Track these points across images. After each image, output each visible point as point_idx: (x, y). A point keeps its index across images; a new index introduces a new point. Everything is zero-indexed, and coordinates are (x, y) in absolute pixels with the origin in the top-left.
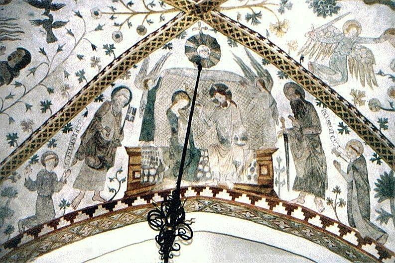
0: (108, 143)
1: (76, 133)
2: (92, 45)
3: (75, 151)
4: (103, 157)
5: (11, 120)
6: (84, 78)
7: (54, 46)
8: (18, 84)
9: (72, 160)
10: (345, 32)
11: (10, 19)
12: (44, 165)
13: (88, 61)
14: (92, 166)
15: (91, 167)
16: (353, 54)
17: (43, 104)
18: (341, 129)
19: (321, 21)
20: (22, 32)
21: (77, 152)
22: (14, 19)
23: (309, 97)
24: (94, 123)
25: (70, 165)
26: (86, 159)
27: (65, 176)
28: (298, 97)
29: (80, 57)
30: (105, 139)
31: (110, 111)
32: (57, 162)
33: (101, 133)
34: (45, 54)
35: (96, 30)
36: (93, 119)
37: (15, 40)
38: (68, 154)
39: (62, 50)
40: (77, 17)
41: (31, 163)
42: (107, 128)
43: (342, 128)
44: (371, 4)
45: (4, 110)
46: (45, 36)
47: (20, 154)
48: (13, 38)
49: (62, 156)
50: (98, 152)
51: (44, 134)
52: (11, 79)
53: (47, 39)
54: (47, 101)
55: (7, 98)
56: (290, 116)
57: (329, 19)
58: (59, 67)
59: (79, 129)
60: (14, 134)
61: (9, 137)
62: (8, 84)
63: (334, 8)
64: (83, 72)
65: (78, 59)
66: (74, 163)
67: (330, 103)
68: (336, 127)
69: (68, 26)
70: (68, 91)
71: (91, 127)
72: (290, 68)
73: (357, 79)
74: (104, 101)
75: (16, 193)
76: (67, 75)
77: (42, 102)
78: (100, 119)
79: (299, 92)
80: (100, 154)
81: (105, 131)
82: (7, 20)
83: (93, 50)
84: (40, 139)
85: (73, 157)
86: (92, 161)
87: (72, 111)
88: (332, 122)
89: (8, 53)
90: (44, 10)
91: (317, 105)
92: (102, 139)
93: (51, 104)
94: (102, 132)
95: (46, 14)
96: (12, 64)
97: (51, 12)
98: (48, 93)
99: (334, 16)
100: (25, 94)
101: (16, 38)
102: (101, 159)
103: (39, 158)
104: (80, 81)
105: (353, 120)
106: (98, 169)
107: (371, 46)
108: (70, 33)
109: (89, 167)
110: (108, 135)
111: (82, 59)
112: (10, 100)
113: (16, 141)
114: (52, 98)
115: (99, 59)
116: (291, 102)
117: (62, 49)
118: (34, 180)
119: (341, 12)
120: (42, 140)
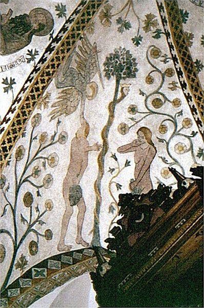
10: (91, 85)
16: (75, 93)
18: (7, 82)
19: (102, 59)
23: (39, 44)
28: (35, 26)
43: (9, 83)
44: (109, 109)
56: (11, 11)
57: (102, 68)
63: (109, 74)
67: (49, 70)
68: (8, 74)
72: (82, 25)
73: (57, 99)
79: (44, 28)
88: (14, 69)
91: (28, 51)
99: (103, 74)
105: (35, 99)
107: (78, 112)
116: (28, 16)
119: (105, 80)
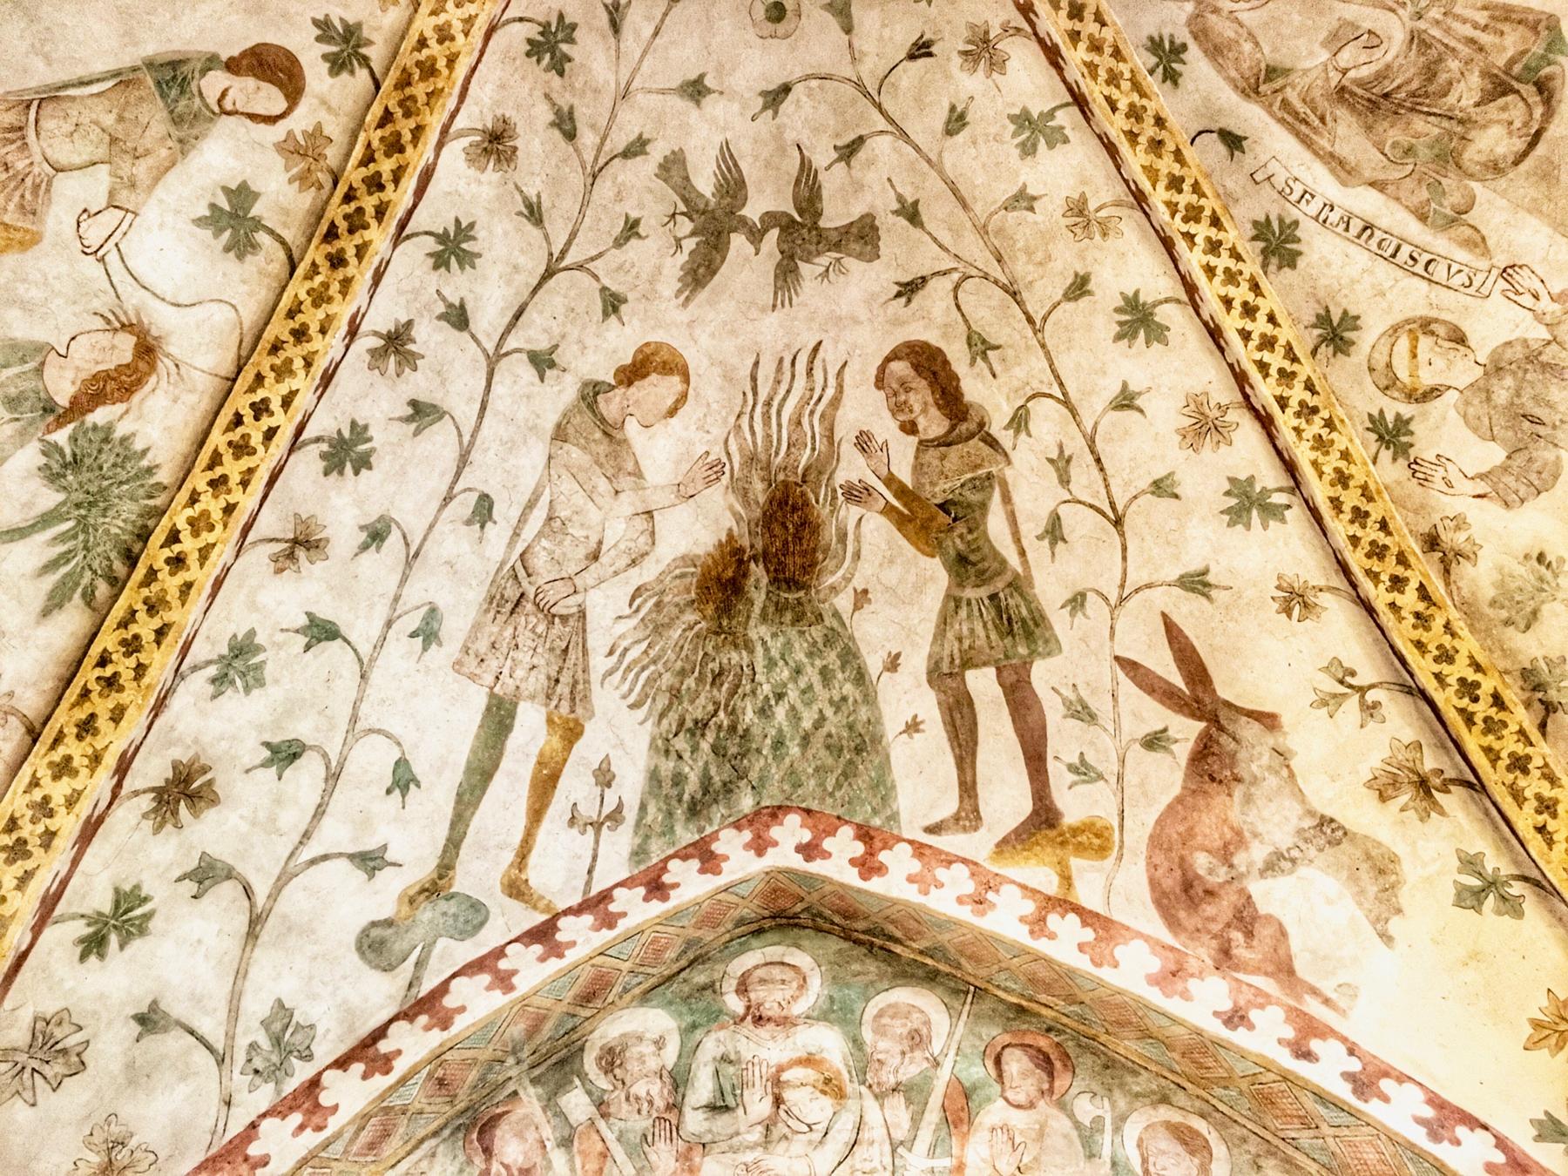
0: (1417, 40)
1: (1313, 208)
2: (912, 57)
3: (1414, 229)
4: (1485, 74)
5: (1162, 488)
6: (1051, 114)
7: (893, 228)
8: (1019, 421)
9: (1462, 255)
11: (754, 379)
12: (1433, 393)
13: (970, 84)
14: (1519, 145)
15: (1524, 155)
17: (1126, 333)
20: (816, 350)
21: (1423, 218)
22: (756, 364)
24: (1285, 104)
25: (1483, 264)
26: (1471, 176)
27: (1536, 297)
29: (956, 121)
30: (1389, 57)
31: (1243, 16)
32: (1441, 330)
33: (1352, 74)
34: (924, 279)
35: (848, 30)
36: (1269, 108)
37: (840, 388)
38: (1422, 266)
39: (916, 203)
40: (787, 106)
41: (1401, 450)
42: (1336, 40)
45: (1113, 508)
46: (850, 262)
47: (1327, 478)
48: (830, 392)
49: (1414, 298)
50: (1451, 99)
51: (1260, 348)
52: (992, 443)
53: (860, 256)
54: (1118, 310)
55: (1065, 481)
58: (983, 230)
59: (1298, 189)
60: (1228, 493)
61: (1237, 515)
62: (1009, 463)
64: (1023, 120)
65: (960, 138)
66: (1478, 243)
69: (822, 156)
70: (1092, 206)
71: (1305, 122)
74: (1183, 36)
75: (1541, 558)
76: (1023, 200)
77: (1119, 337)
78: (1272, 72)
80: (1466, 92)
81: (1345, 58)
82: (755, 393)
83: (930, 55)
84: (1281, 371)
85: (1440, 244)
86: (1493, 140)
87: (1180, 191)
89: (885, 428)
90: (738, 241)
92: (1381, 76)
93: (1136, 293)
94: (1345, 72)
95: (756, 236)
96: (934, 424)
97: (753, 211)
98: (1084, 302)
100: (1066, 402)
101: (832, 382)
102: (1499, 87)
103: (1394, 408)
104: (1057, 138)
106: (1549, 114)
108: (849, 151)
109: (1523, 167)
110: (1373, 41)
111: (962, 117)
112: (1074, 471)
113: (1265, 492)
114: (1110, 284)
115: (972, 27)
117: (910, 200)
118: (1495, 454)
120: (1287, 365)
